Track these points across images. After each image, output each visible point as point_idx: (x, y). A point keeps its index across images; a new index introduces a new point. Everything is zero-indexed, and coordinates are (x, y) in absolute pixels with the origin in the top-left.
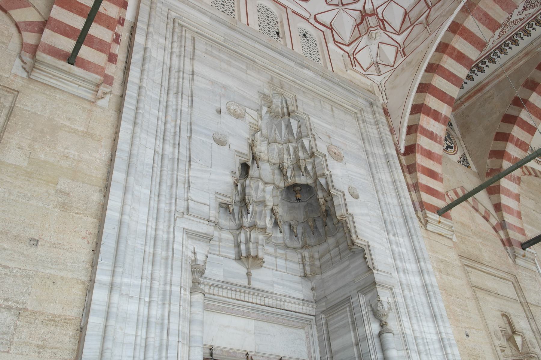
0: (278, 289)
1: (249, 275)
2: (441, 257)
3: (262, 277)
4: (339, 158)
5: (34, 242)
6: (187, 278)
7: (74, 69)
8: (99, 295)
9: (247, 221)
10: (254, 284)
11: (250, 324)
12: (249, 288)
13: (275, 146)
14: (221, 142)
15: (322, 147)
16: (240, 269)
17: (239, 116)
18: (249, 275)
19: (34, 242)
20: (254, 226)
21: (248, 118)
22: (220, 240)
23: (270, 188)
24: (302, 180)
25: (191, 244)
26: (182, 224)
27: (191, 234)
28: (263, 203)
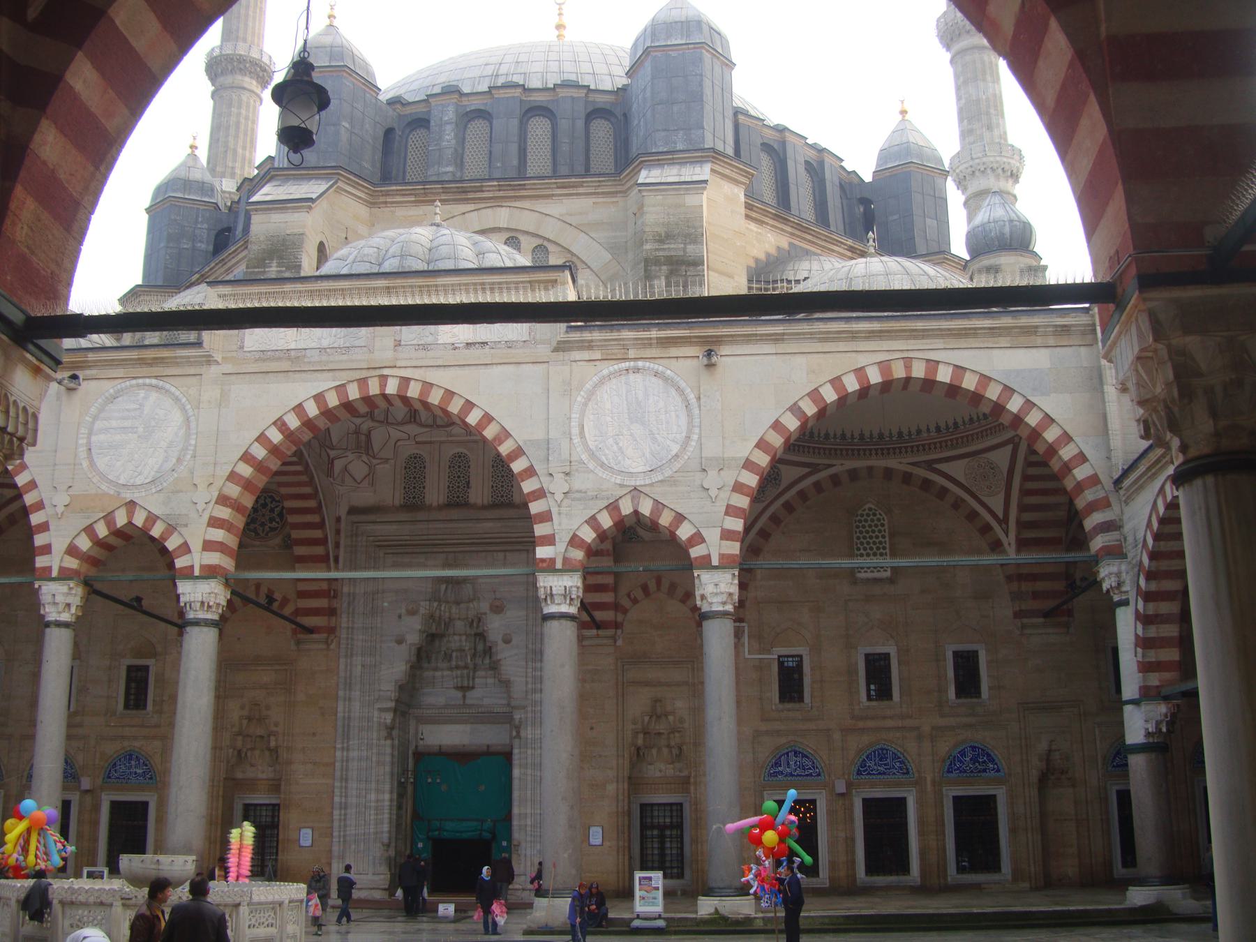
0: (486, 701)
1: (464, 697)
2: (590, 667)
3: (473, 696)
4: (498, 609)
5: (314, 734)
6: (384, 733)
7: (314, 636)
8: (338, 754)
9: (454, 663)
10: (468, 702)
11: (468, 728)
12: (465, 705)
13: (462, 605)
14: (400, 641)
15: (484, 606)
16: (459, 694)
17: (412, 613)
18: (464, 697)
19: (314, 734)
20: (457, 667)
21: (422, 611)
22: (443, 677)
23: (464, 638)
24: (480, 630)
25: (384, 715)
26: (378, 706)
27: (381, 710)
28: (461, 650)
